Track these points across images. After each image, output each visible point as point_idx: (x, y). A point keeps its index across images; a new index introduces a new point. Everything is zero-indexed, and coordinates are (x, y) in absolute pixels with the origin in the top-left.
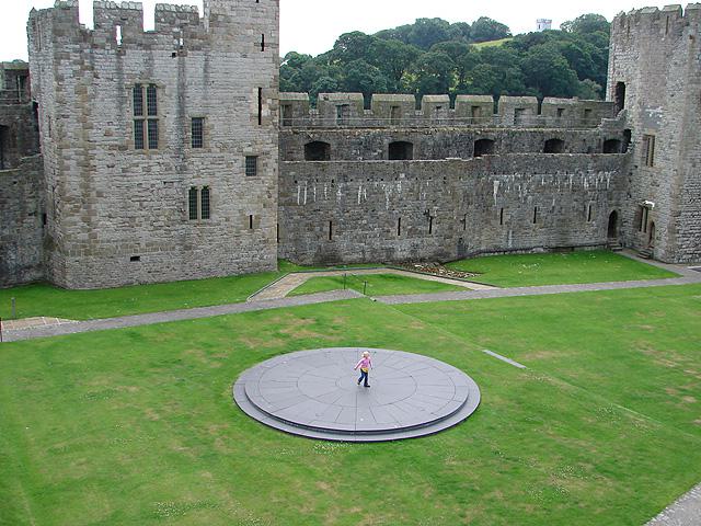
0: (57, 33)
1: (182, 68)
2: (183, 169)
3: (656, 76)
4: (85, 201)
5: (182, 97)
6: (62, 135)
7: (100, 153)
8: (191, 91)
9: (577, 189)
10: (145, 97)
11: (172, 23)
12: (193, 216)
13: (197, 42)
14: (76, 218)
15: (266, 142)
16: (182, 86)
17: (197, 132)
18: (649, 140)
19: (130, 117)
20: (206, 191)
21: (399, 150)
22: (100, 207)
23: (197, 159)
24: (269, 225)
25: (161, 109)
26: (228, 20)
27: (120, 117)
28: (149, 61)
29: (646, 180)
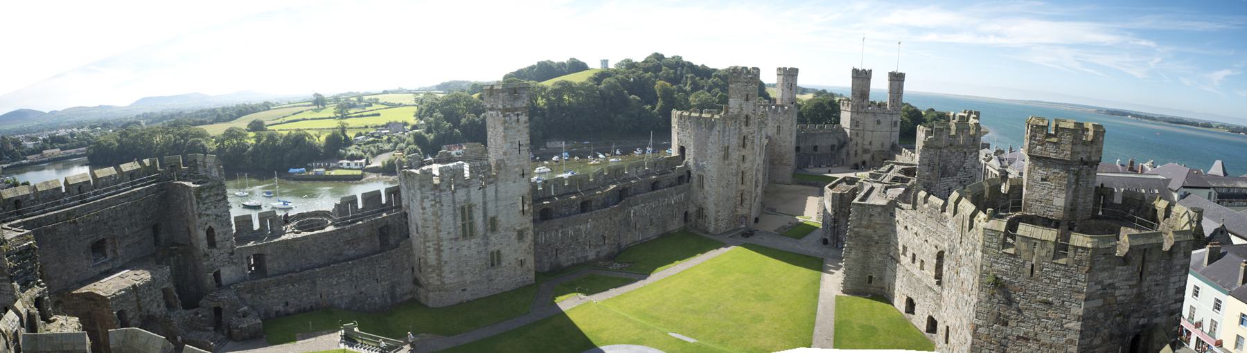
0: (422, 186)
1: (484, 194)
2: (487, 244)
5: (485, 209)
6: (426, 236)
7: (445, 243)
9: (669, 205)
10: (466, 212)
15: (527, 222)
16: (485, 203)
17: (493, 225)
18: (701, 178)
19: (459, 223)
20: (498, 252)
23: (493, 238)
24: (530, 262)
25: (475, 216)
26: (506, 165)
28: (468, 194)
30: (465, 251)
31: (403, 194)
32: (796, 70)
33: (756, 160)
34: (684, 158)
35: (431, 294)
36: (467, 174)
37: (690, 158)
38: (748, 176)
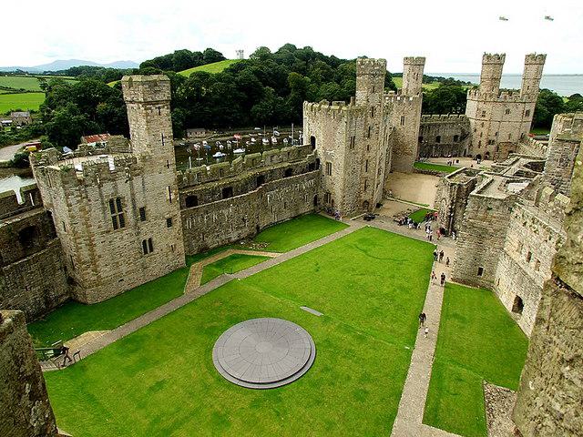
0: (64, 183)
1: (132, 185)
3: (330, 136)
4: (93, 261)
5: (133, 200)
6: (75, 233)
8: (137, 196)
10: (116, 204)
11: (124, 166)
12: (146, 252)
13: (137, 172)
14: (89, 271)
15: (175, 211)
16: (133, 194)
19: (109, 216)
20: (150, 240)
21: (227, 192)
22: (101, 262)
23: (144, 227)
24: (181, 247)
27: (105, 218)
28: (115, 187)
29: (329, 182)
30: (117, 243)
31: (43, 192)
32: (425, 58)
33: (380, 150)
34: (314, 147)
35: (88, 291)
36: (112, 168)
37: (319, 148)
38: (371, 164)
